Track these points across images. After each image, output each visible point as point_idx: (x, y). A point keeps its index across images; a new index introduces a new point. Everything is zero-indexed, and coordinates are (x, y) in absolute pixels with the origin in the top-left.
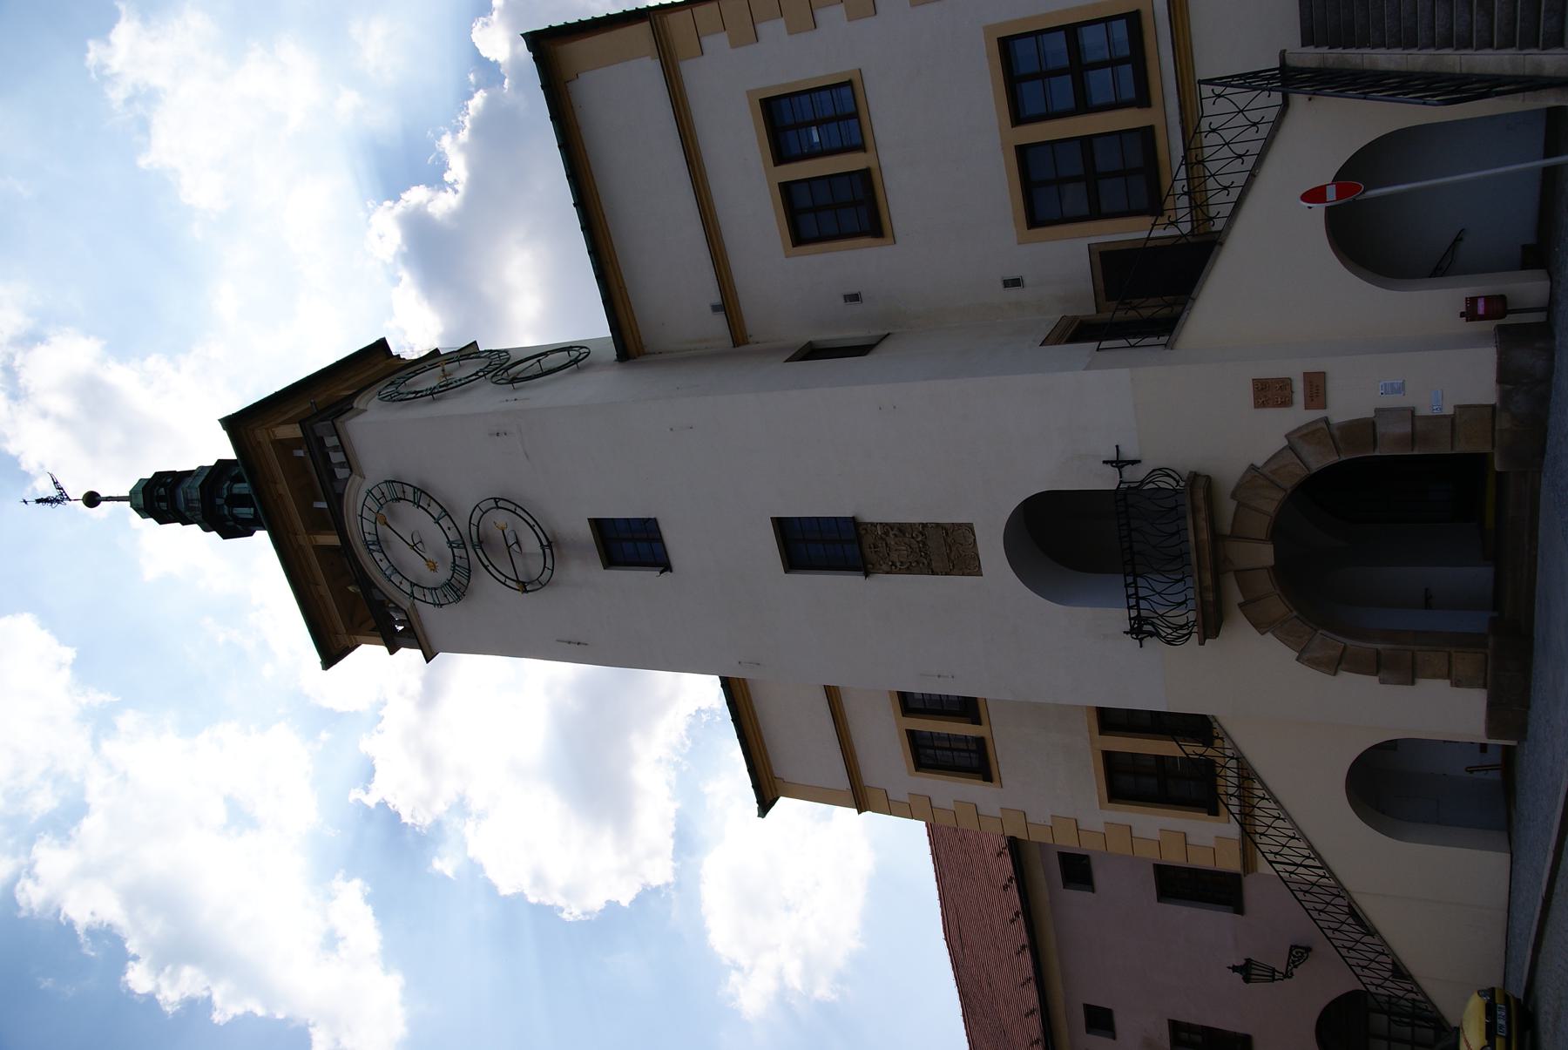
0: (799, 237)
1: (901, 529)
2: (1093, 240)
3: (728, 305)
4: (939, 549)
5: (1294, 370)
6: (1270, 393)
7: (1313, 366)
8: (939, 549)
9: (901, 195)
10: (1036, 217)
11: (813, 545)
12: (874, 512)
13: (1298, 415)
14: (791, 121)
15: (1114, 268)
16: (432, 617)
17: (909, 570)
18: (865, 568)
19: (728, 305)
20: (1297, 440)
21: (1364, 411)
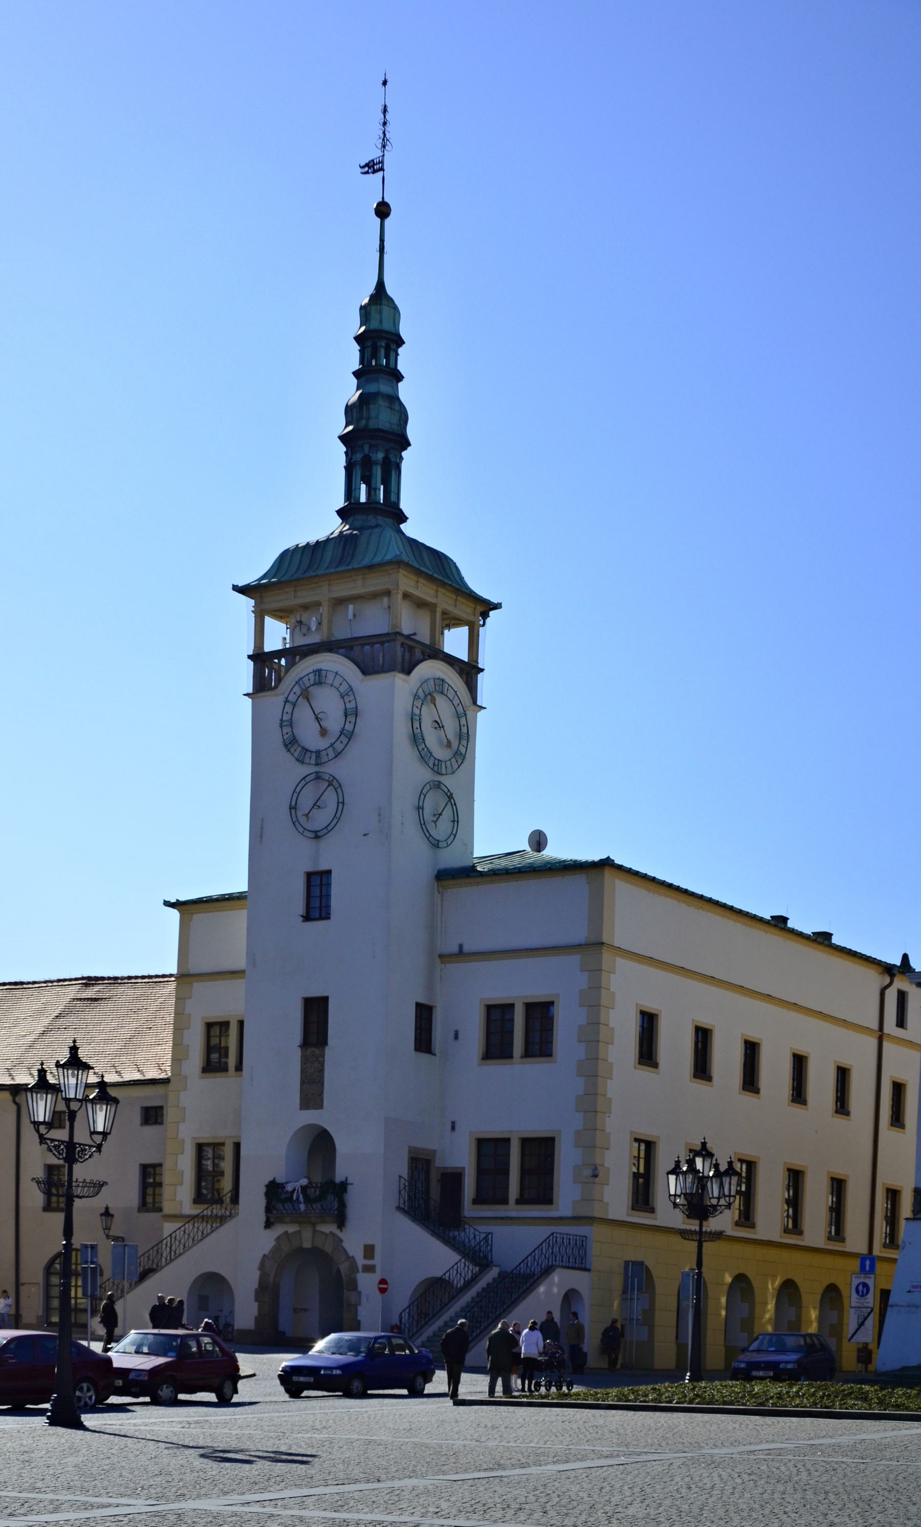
0: (490, 1008)
1: (321, 1071)
2: (467, 1170)
3: (461, 954)
4: (312, 1091)
5: (377, 1261)
6: (369, 1251)
7: (378, 1270)
8: (312, 1091)
9: (498, 1070)
10: (481, 1143)
11: (316, 1011)
12: (330, 1053)
13: (361, 1261)
14: (541, 1013)
15: (453, 1179)
16: (274, 701)
17: (302, 1071)
18: (305, 1044)
19: (461, 954)
20: (352, 1260)
21: (360, 1287)
